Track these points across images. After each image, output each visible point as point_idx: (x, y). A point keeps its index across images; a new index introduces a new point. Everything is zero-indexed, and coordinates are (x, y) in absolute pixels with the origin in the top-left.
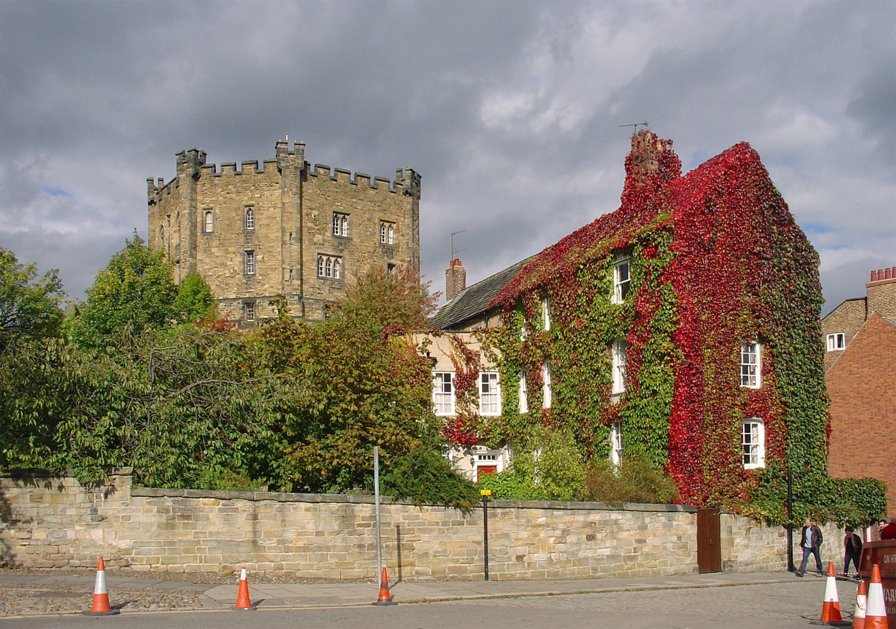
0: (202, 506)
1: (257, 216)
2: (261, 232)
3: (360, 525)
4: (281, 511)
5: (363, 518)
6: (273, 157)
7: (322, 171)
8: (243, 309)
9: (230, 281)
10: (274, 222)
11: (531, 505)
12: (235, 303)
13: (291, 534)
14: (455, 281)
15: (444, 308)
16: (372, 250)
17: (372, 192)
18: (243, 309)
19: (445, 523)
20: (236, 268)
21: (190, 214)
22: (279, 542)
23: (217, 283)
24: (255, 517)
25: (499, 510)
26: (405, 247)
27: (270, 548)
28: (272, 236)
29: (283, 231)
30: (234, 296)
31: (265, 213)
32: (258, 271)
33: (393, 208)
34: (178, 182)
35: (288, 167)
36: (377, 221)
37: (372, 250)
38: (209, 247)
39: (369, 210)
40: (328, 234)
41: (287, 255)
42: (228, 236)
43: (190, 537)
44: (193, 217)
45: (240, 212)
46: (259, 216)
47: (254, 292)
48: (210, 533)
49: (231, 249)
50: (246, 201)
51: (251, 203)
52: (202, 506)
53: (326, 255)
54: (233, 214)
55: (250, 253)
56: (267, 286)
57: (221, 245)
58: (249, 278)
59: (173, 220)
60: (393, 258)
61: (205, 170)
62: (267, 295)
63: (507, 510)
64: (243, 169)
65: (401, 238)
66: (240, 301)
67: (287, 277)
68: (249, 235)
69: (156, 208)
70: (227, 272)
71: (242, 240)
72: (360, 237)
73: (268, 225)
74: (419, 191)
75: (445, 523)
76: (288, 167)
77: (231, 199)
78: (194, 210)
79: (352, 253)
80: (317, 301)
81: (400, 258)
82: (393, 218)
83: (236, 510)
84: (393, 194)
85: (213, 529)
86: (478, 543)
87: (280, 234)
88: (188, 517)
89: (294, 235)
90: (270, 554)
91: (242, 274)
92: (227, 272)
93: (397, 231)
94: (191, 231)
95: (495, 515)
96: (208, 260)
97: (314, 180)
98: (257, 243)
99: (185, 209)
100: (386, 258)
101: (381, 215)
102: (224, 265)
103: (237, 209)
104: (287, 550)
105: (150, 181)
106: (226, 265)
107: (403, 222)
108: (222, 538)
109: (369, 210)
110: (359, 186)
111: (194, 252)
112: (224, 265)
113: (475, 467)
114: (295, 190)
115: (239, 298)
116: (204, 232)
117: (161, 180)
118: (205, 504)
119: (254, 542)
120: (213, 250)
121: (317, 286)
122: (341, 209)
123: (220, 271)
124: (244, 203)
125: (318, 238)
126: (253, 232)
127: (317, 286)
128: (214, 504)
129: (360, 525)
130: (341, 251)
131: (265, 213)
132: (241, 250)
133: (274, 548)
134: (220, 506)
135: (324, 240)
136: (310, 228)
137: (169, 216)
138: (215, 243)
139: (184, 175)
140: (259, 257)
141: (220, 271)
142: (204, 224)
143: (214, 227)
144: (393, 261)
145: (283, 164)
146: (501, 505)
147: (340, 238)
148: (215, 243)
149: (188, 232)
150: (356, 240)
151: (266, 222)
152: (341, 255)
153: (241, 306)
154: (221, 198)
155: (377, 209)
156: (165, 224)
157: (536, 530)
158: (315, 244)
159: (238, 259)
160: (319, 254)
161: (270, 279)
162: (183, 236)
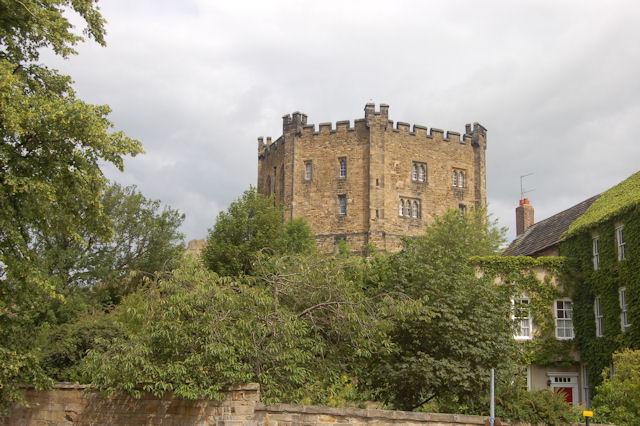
1: (348, 167)
7: (403, 128)
15: (515, 241)
17: (445, 144)
30: (327, 233)
32: (348, 212)
33: (463, 157)
35: (374, 125)
36: (449, 168)
37: (445, 193)
40: (408, 180)
47: (347, 228)
54: (329, 165)
56: (356, 224)
59: (278, 171)
71: (335, 186)
76: (374, 125)
80: (398, 236)
82: (463, 166)
89: (380, 181)
93: (465, 177)
96: (307, 203)
97: (397, 136)
98: (348, 188)
101: (453, 163)
103: (332, 161)
105: (261, 140)
113: (552, 389)
114: (380, 144)
115: (332, 235)
117: (269, 139)
125: (400, 183)
130: (419, 194)
139: (288, 135)
140: (350, 201)
144: (464, 203)
150: (431, 185)
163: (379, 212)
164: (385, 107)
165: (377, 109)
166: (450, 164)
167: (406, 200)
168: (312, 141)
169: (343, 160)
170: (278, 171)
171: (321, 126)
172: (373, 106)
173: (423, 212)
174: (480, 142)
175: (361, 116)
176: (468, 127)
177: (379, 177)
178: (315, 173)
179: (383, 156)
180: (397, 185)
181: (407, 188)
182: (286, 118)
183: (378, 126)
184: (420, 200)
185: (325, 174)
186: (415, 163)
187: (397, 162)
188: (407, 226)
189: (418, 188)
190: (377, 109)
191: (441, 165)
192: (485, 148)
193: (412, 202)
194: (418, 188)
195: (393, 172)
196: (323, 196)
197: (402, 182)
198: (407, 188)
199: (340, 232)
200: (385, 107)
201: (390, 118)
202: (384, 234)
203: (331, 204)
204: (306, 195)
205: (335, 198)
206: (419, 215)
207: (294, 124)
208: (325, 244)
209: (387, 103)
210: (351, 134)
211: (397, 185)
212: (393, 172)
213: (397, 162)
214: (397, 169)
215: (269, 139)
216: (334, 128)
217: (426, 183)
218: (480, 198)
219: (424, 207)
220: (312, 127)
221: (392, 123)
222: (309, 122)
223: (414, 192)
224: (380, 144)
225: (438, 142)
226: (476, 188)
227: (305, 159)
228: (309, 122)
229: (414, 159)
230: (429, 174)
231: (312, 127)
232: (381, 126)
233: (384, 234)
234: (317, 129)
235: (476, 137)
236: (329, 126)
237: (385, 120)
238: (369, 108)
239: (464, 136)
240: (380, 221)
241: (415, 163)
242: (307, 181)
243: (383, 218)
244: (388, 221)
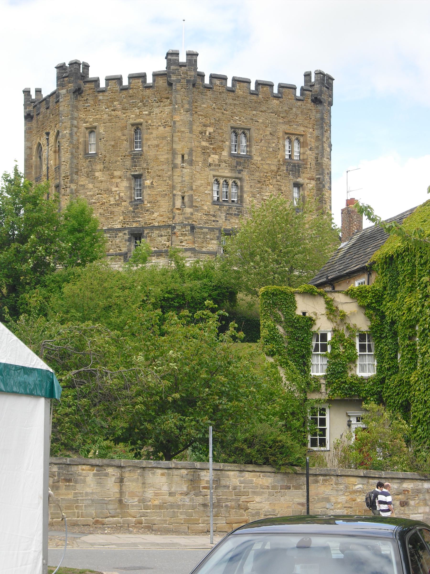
0: (80, 471)
1: (145, 136)
2: (150, 153)
3: (204, 488)
4: (142, 476)
5: (208, 482)
7: (218, 82)
8: (129, 240)
9: (116, 209)
10: (164, 142)
11: (349, 473)
12: (120, 234)
13: (149, 494)
14: (350, 222)
16: (274, 168)
17: (276, 102)
18: (129, 240)
19: (274, 487)
20: (122, 194)
21: (71, 134)
22: (139, 501)
23: (101, 211)
24: (121, 480)
25: (321, 478)
26: (313, 163)
27: (133, 506)
29: (174, 153)
30: (119, 226)
31: (155, 132)
34: (58, 96)
35: (179, 81)
36: (281, 134)
37: (274, 168)
38: (93, 171)
39: (271, 123)
40: (225, 153)
41: (177, 179)
42: (114, 159)
43: (71, 497)
44: (75, 138)
45: (126, 132)
48: (87, 493)
50: (133, 118)
51: (138, 121)
52: (80, 471)
53: (223, 177)
54: (119, 134)
55: (138, 177)
56: (156, 215)
57: (106, 169)
58: (137, 204)
59: (52, 139)
60: (299, 176)
61: (88, 85)
62: (156, 224)
63: (328, 477)
64: (130, 83)
65: (309, 152)
66: (126, 232)
67: (178, 203)
68: (136, 158)
69: (34, 123)
70: (112, 199)
71: (128, 163)
72: (261, 154)
73: (158, 146)
74: (331, 96)
75: (274, 487)
76: (179, 81)
77: (116, 116)
78: (75, 129)
79: (251, 173)
80: (212, 230)
81: (308, 176)
83: (107, 475)
84: (299, 103)
85: (89, 490)
86: (302, 504)
87: (170, 156)
88: (69, 481)
89: (186, 157)
90: (132, 511)
91: (128, 201)
92: (112, 199)
93: (302, 145)
94: (72, 154)
95: (317, 482)
96: (91, 186)
97: (209, 93)
98: (145, 166)
99: (66, 128)
100: (291, 177)
101: (286, 128)
102: (109, 191)
104: (146, 507)
105: (27, 92)
106: (111, 192)
107: (311, 134)
108: (96, 497)
109: (271, 123)
110: (260, 96)
111: (75, 177)
112: (109, 191)
114: (187, 106)
115: (125, 229)
116: (86, 153)
118: (83, 470)
119: (120, 501)
120: (97, 174)
121: (212, 213)
122: (239, 124)
124: (132, 121)
125: (214, 158)
126: (141, 154)
127: (212, 213)
128: (90, 470)
129: (204, 488)
130: (240, 172)
131: (155, 132)
132: (128, 174)
133: (136, 506)
134: (95, 471)
135: (220, 161)
136: (204, 148)
137: (48, 134)
139: (63, 91)
140: (148, 182)
142: (86, 145)
143: (98, 148)
144: (300, 180)
145: (174, 78)
146: (323, 472)
147: (238, 156)
149: (68, 155)
150: (257, 158)
151: (156, 142)
152: (240, 176)
153: (127, 237)
154: (105, 116)
155: (281, 121)
156: (43, 141)
157: (354, 496)
159: (125, 184)
160: (214, 176)
161: (159, 207)
162: (63, 159)
163: (186, 199)
165: (183, 59)
166: (282, 128)
167: (221, 181)
168: (97, 102)
169: (137, 127)
170: (52, 139)
171: (108, 80)
172: (177, 54)
173: (245, 196)
174: (324, 97)
176: (307, 75)
177: (186, 151)
178: (101, 145)
179: (191, 124)
180: (210, 160)
181: (223, 165)
182: (61, 68)
183: (184, 82)
184: (240, 179)
185: (113, 146)
186: (235, 130)
187: (210, 130)
188: (223, 215)
189: (238, 164)
190: (183, 59)
191: (269, 130)
192: (331, 104)
193: (230, 182)
194: (238, 164)
195: (204, 144)
197: (217, 157)
198: (223, 165)
199: (134, 225)
200: (192, 56)
201: (200, 69)
202: (193, 228)
203: (122, 187)
204: (90, 175)
205: (128, 179)
206: (241, 199)
207: (73, 75)
208: (118, 240)
210: (148, 92)
211: (210, 160)
212: (204, 144)
213: (210, 130)
214: (210, 139)
215: (38, 91)
216: (125, 82)
217: (249, 157)
218: (322, 174)
219: (245, 189)
220: (96, 81)
221: (202, 76)
222: (92, 75)
223: (233, 169)
224: (187, 106)
225: (266, 99)
226: (317, 158)
227: (88, 125)
228: (92, 75)
229: (232, 123)
230: (253, 142)
231: (96, 81)
232: (188, 81)
233: (193, 228)
234: (103, 84)
235: (319, 91)
236: (119, 79)
237: (193, 73)
239: (302, 89)
240: (188, 210)
241: (235, 130)
242: (93, 156)
243: (191, 206)
244: (196, 208)
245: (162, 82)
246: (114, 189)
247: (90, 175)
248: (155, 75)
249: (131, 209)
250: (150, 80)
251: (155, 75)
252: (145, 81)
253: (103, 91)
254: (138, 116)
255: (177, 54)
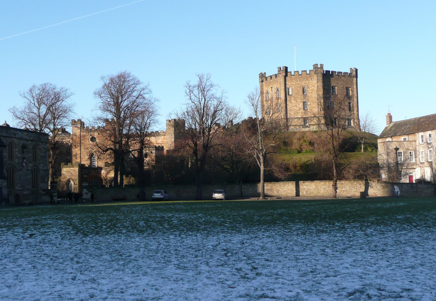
6: (312, 68)
17: (343, 78)
20: (301, 107)
28: (313, 96)
30: (300, 117)
35: (318, 73)
42: (297, 96)
46: (308, 90)
49: (298, 101)
54: (299, 89)
71: (302, 98)
73: (312, 92)
99: (282, 87)
106: (297, 106)
114: (321, 81)
115: (302, 117)
123: (295, 108)
131: (310, 88)
137: (272, 88)
138: (293, 99)
140: (309, 103)
141: (295, 108)
143: (292, 93)
148: (293, 99)
151: (311, 91)
154: (294, 83)
158: (327, 98)
164: (322, 65)
165: (319, 66)
175: (312, 68)
176: (351, 69)
180: (327, 97)
183: (320, 73)
190: (319, 66)
196: (297, 101)
197: (328, 95)
200: (322, 65)
209: (323, 64)
213: (326, 87)
220: (291, 72)
231: (291, 72)
234: (293, 73)
238: (315, 66)
245: (312, 73)
246: (298, 105)
247: (290, 101)
248: (310, 71)
249: (304, 111)
250: (308, 72)
251: (310, 71)
252: (306, 73)
253: (294, 75)
254: (305, 83)
255: (317, 65)
